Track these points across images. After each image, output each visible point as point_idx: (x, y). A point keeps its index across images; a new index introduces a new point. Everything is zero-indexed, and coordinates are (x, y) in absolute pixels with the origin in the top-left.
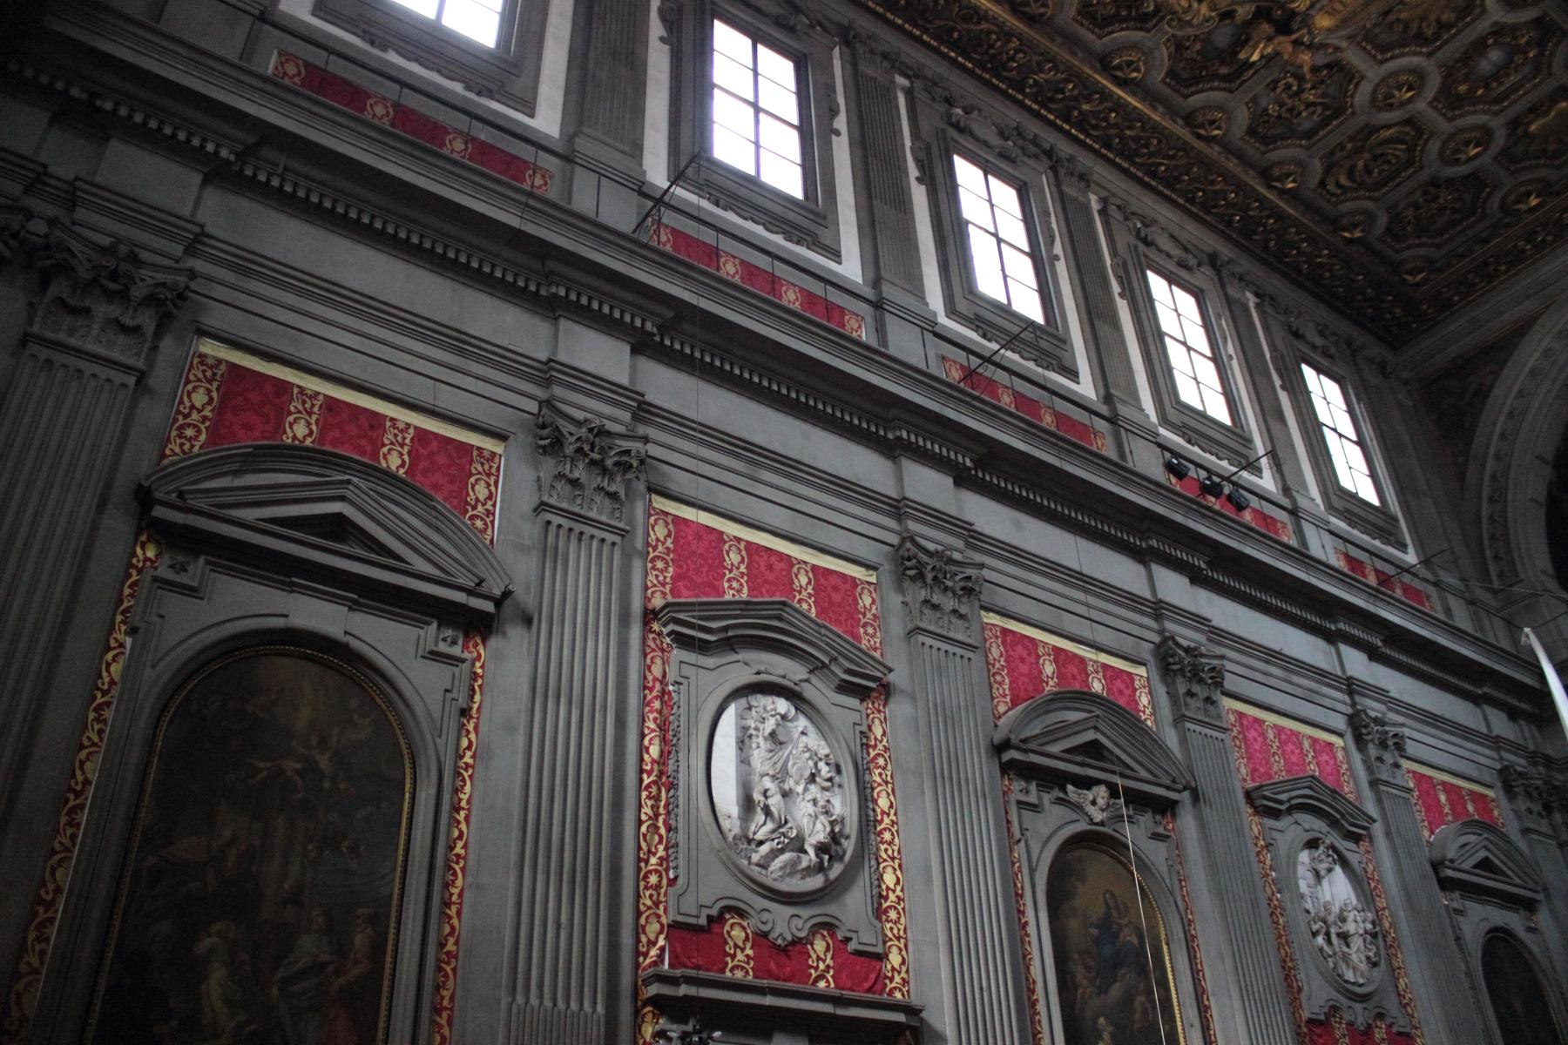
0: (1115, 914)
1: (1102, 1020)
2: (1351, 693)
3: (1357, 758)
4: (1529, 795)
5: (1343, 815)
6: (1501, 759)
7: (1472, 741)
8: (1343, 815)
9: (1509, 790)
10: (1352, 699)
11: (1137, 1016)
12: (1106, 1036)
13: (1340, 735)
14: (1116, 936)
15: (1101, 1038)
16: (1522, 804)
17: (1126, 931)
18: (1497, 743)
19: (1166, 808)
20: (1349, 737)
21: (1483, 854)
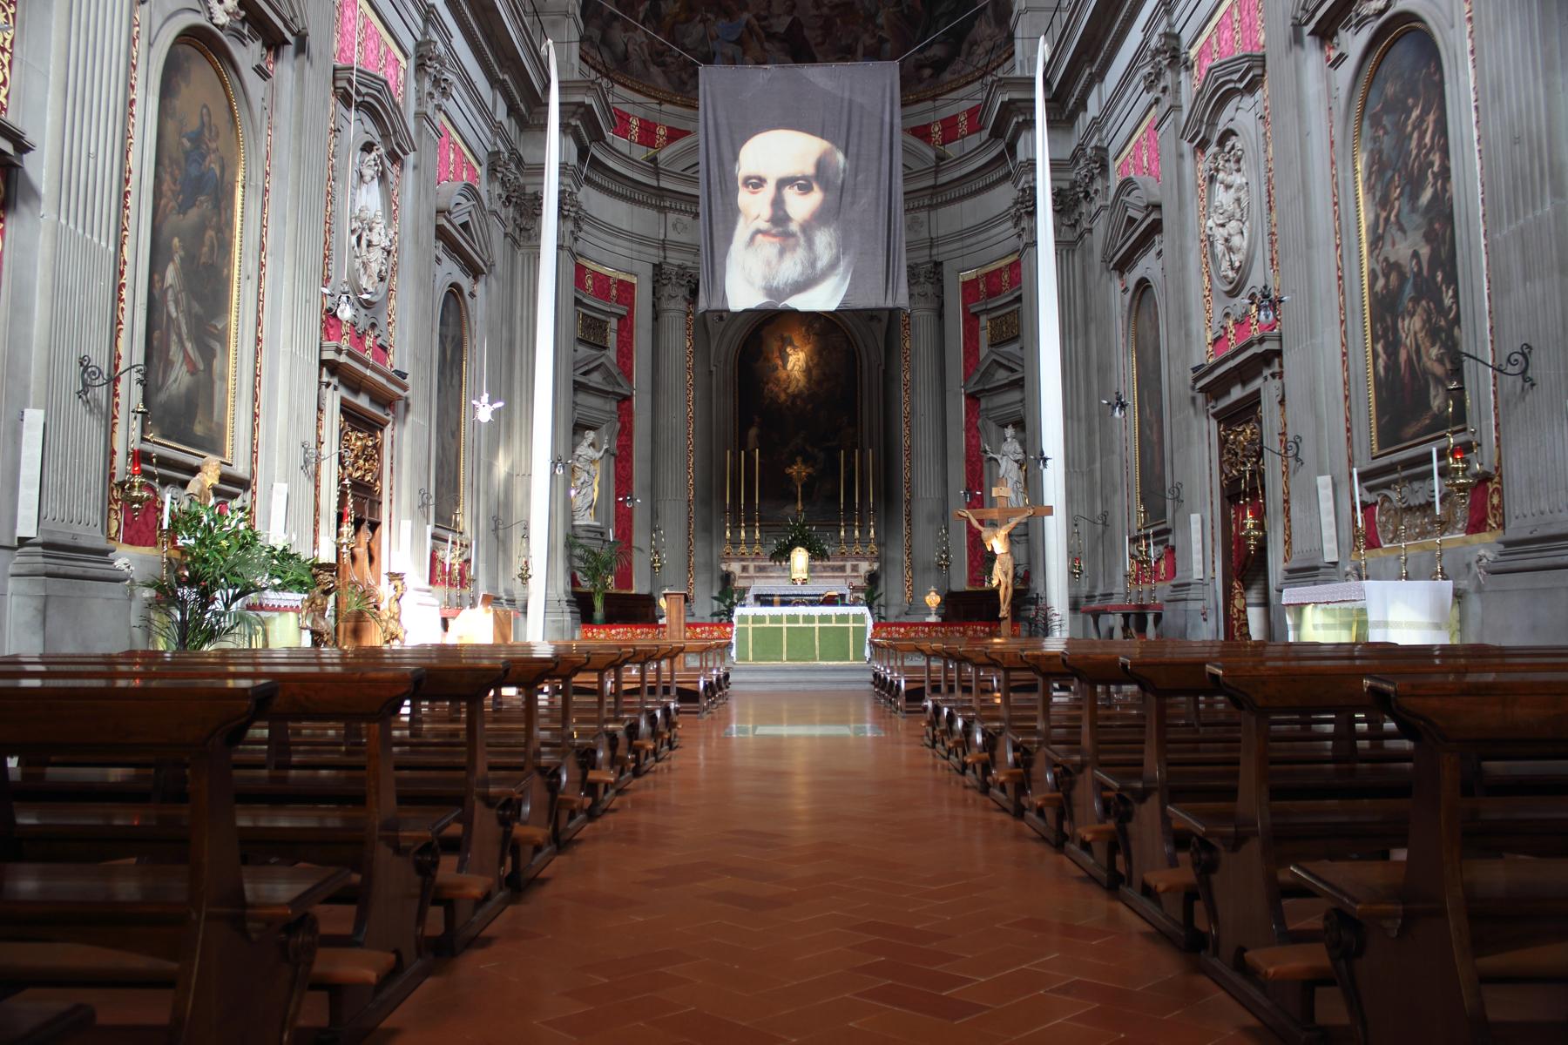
0: (206, 133)
1: (176, 241)
2: (426, 20)
3: (413, 84)
4: (503, 183)
5: (395, 132)
6: (495, 144)
7: (483, 118)
8: (395, 132)
9: (492, 171)
10: (425, 27)
11: (205, 249)
12: (177, 258)
13: (406, 56)
14: (204, 157)
15: (172, 259)
16: (497, 189)
17: (213, 156)
18: (496, 128)
19: (274, 43)
20: (412, 61)
21: (466, 218)
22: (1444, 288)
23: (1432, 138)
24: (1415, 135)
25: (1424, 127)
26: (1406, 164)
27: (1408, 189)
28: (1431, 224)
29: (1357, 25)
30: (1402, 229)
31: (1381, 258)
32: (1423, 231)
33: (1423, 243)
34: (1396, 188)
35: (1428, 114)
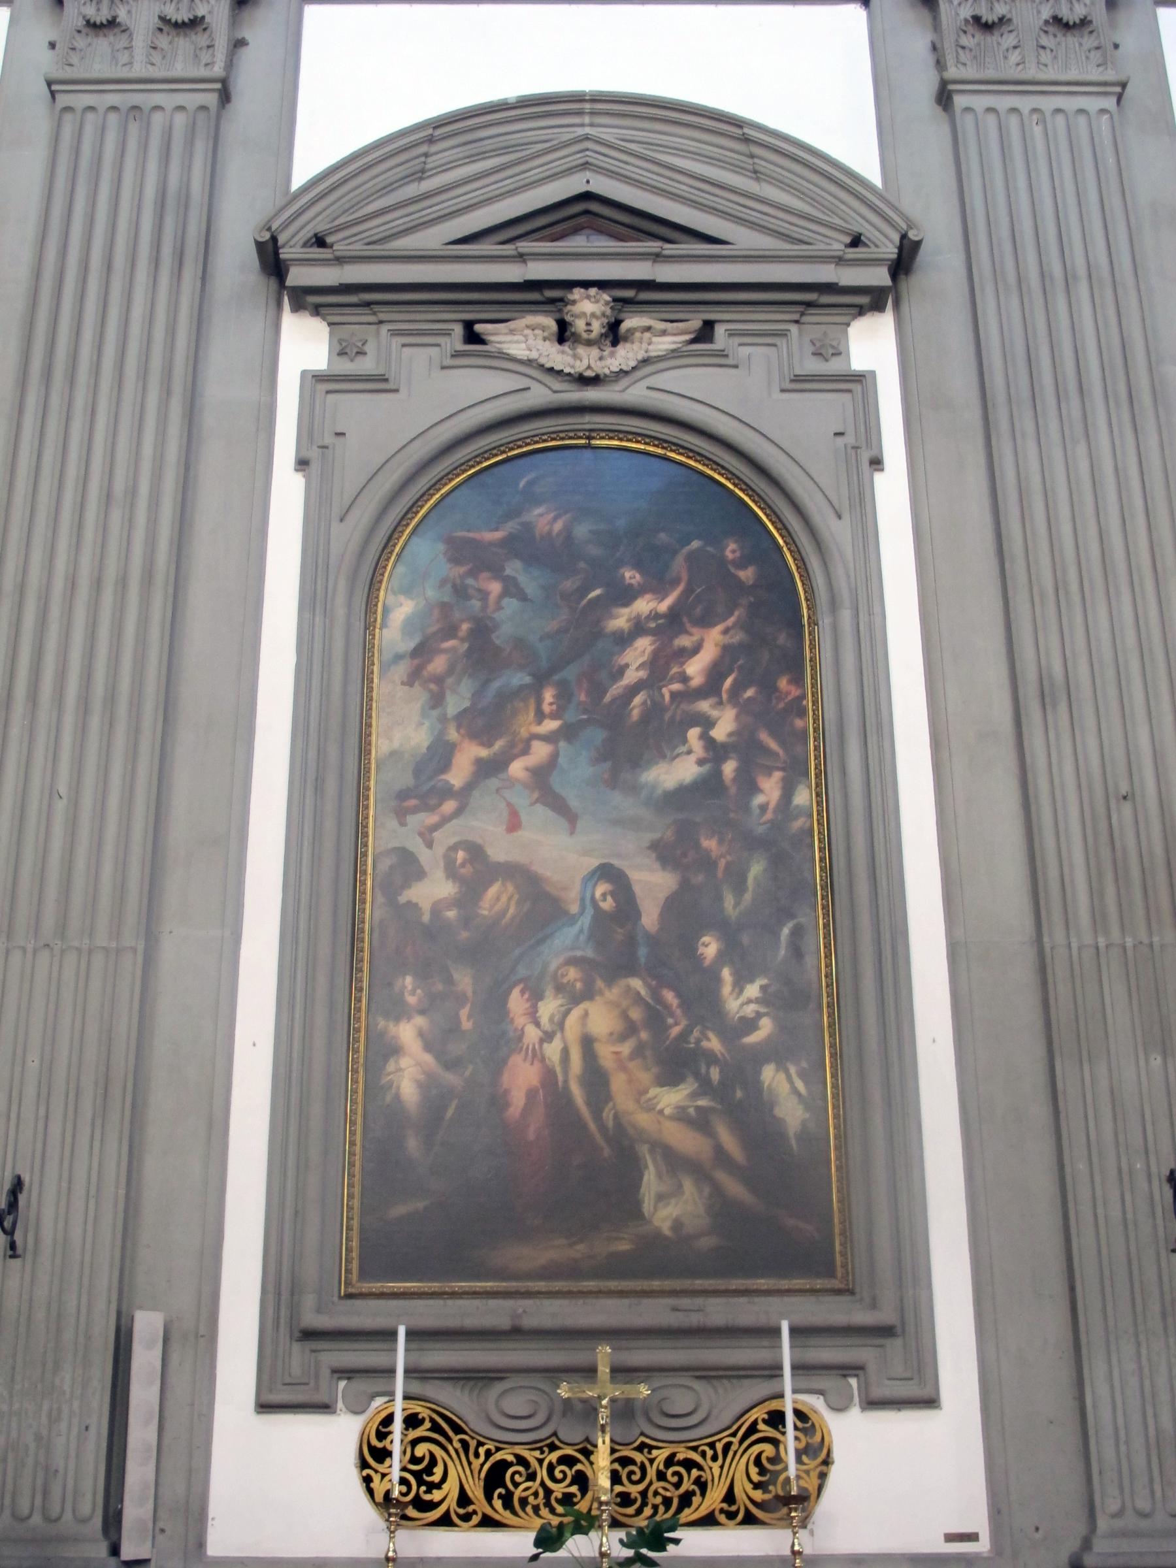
22: (726, 974)
23: (715, 675)
24: (644, 646)
25: (684, 641)
26: (598, 690)
27: (598, 735)
28: (686, 833)
29: (457, 355)
30: (559, 806)
31: (445, 838)
32: (649, 837)
33: (649, 860)
34: (540, 716)
35: (705, 621)
